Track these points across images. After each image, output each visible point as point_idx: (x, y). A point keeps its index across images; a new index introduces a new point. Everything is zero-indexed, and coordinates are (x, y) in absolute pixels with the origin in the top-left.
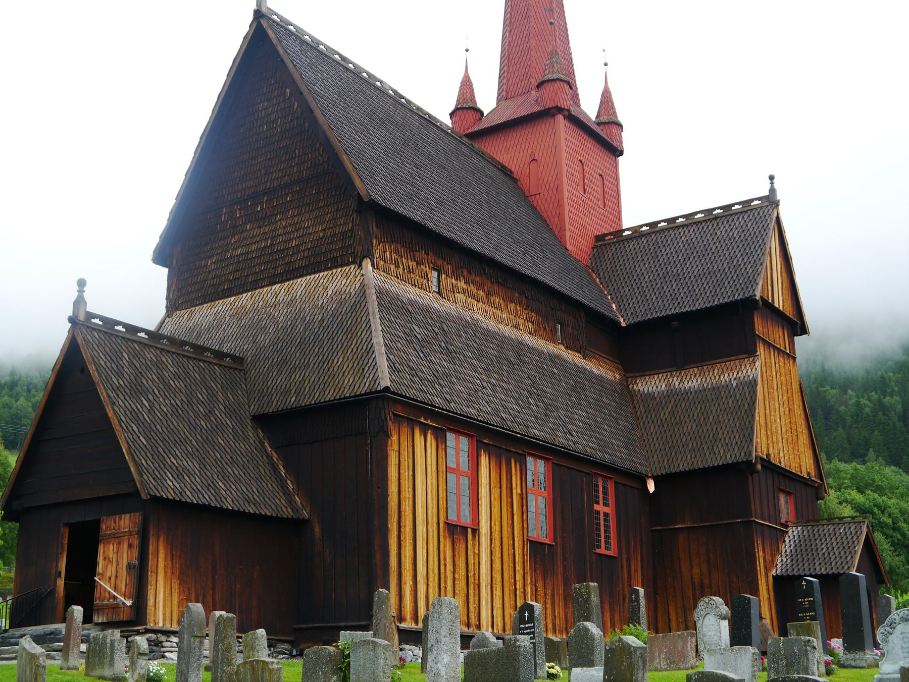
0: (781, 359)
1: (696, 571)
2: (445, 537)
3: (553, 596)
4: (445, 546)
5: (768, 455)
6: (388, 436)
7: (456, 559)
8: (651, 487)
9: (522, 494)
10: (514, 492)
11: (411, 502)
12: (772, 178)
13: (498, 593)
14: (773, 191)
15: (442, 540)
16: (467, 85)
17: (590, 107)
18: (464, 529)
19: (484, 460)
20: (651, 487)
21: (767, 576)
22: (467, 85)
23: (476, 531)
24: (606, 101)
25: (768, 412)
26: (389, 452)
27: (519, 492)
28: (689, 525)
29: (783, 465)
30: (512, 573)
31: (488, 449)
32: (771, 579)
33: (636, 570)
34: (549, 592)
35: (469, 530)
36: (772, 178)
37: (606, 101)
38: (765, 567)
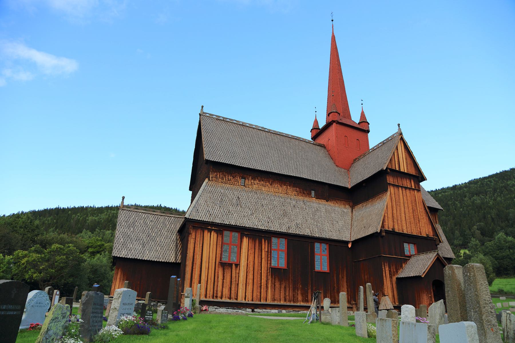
0: (404, 192)
1: (366, 277)
2: (219, 267)
3: (285, 288)
4: (218, 270)
5: (393, 229)
6: (190, 234)
7: (225, 275)
8: (350, 246)
9: (268, 251)
10: (263, 250)
11: (200, 256)
12: (399, 125)
13: (250, 288)
14: (400, 129)
15: (217, 268)
16: (316, 122)
17: (356, 118)
18: (230, 265)
19: (245, 240)
20: (350, 246)
21: (391, 277)
22: (316, 122)
23: (237, 265)
24: (363, 115)
25: (395, 212)
26: (189, 239)
27: (266, 250)
28: (364, 259)
29: (405, 232)
30: (259, 279)
31: (247, 236)
32: (394, 279)
33: (343, 277)
34: (283, 286)
35: (234, 265)
36: (399, 125)
37: (363, 115)
38: (390, 274)
